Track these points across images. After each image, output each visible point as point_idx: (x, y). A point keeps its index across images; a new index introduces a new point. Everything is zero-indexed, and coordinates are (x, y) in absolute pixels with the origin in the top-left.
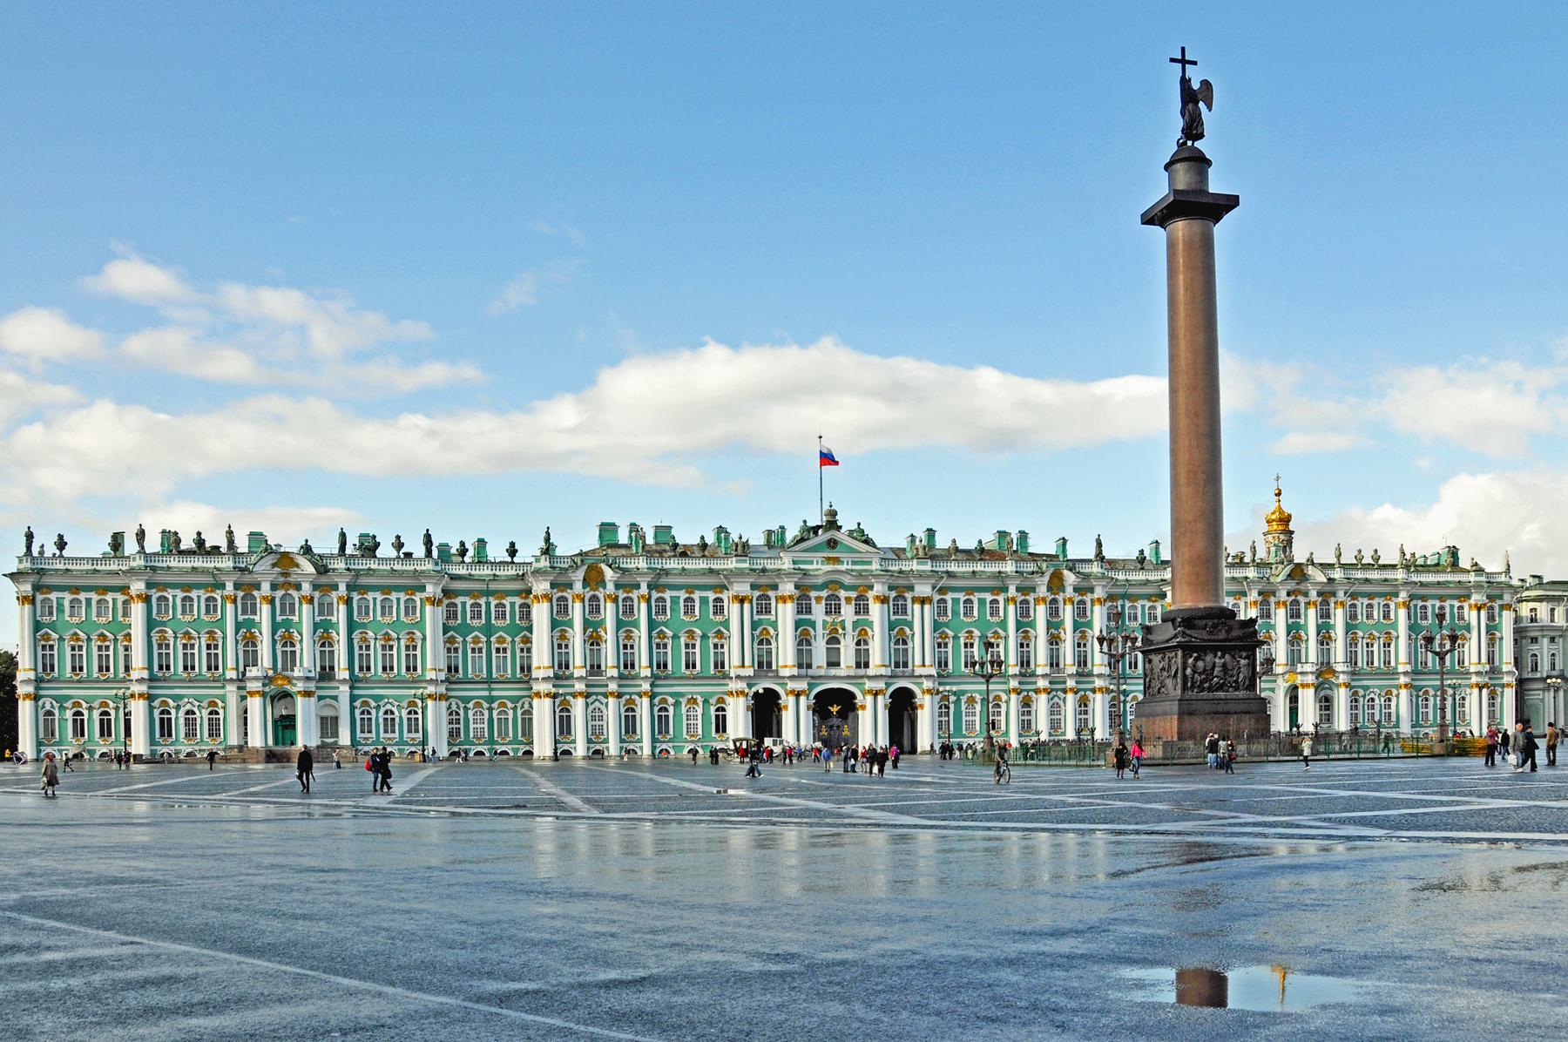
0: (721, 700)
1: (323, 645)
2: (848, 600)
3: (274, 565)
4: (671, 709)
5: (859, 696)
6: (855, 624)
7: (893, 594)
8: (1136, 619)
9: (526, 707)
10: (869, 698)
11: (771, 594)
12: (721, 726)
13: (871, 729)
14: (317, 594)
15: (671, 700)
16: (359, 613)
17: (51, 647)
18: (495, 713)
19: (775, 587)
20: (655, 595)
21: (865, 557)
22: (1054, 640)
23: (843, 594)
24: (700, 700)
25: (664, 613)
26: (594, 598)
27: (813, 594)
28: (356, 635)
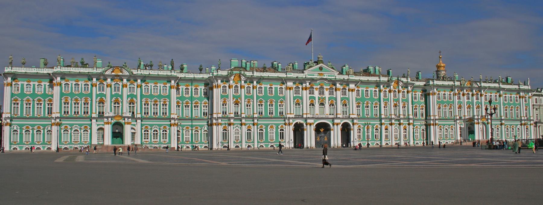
0: (282, 126)
1: (130, 104)
2: (327, 89)
3: (112, 72)
5: (331, 125)
8: (416, 98)
10: (335, 126)
12: (282, 136)
14: (128, 84)
16: (145, 91)
17: (18, 104)
18: (194, 131)
20: (258, 86)
22: (395, 106)
23: (325, 87)
24: (274, 126)
25: (262, 93)
26: (236, 86)
28: (144, 100)
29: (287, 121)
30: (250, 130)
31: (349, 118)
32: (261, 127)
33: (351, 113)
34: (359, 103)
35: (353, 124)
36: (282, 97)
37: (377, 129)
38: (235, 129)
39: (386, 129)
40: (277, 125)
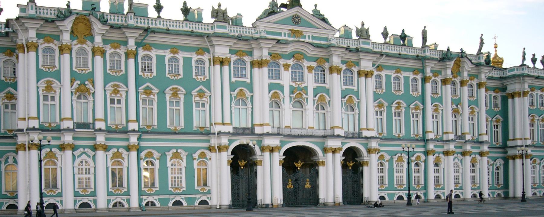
0: (203, 155)
2: (310, 69)
4: (157, 163)
6: (316, 91)
7: (344, 67)
9: (11, 161)
10: (330, 155)
11: (247, 59)
13: (330, 183)
15: (156, 155)
19: (250, 54)
21: (323, 33)
22: (456, 113)
24: (184, 155)
25: (150, 70)
27: (282, 62)
29: (214, 142)
30: (120, 163)
31: (359, 136)
32: (150, 155)
33: (364, 126)
34: (380, 105)
35: (369, 151)
36: (202, 83)
37: (417, 165)
38: (78, 161)
39: (436, 165)
40: (190, 152)
